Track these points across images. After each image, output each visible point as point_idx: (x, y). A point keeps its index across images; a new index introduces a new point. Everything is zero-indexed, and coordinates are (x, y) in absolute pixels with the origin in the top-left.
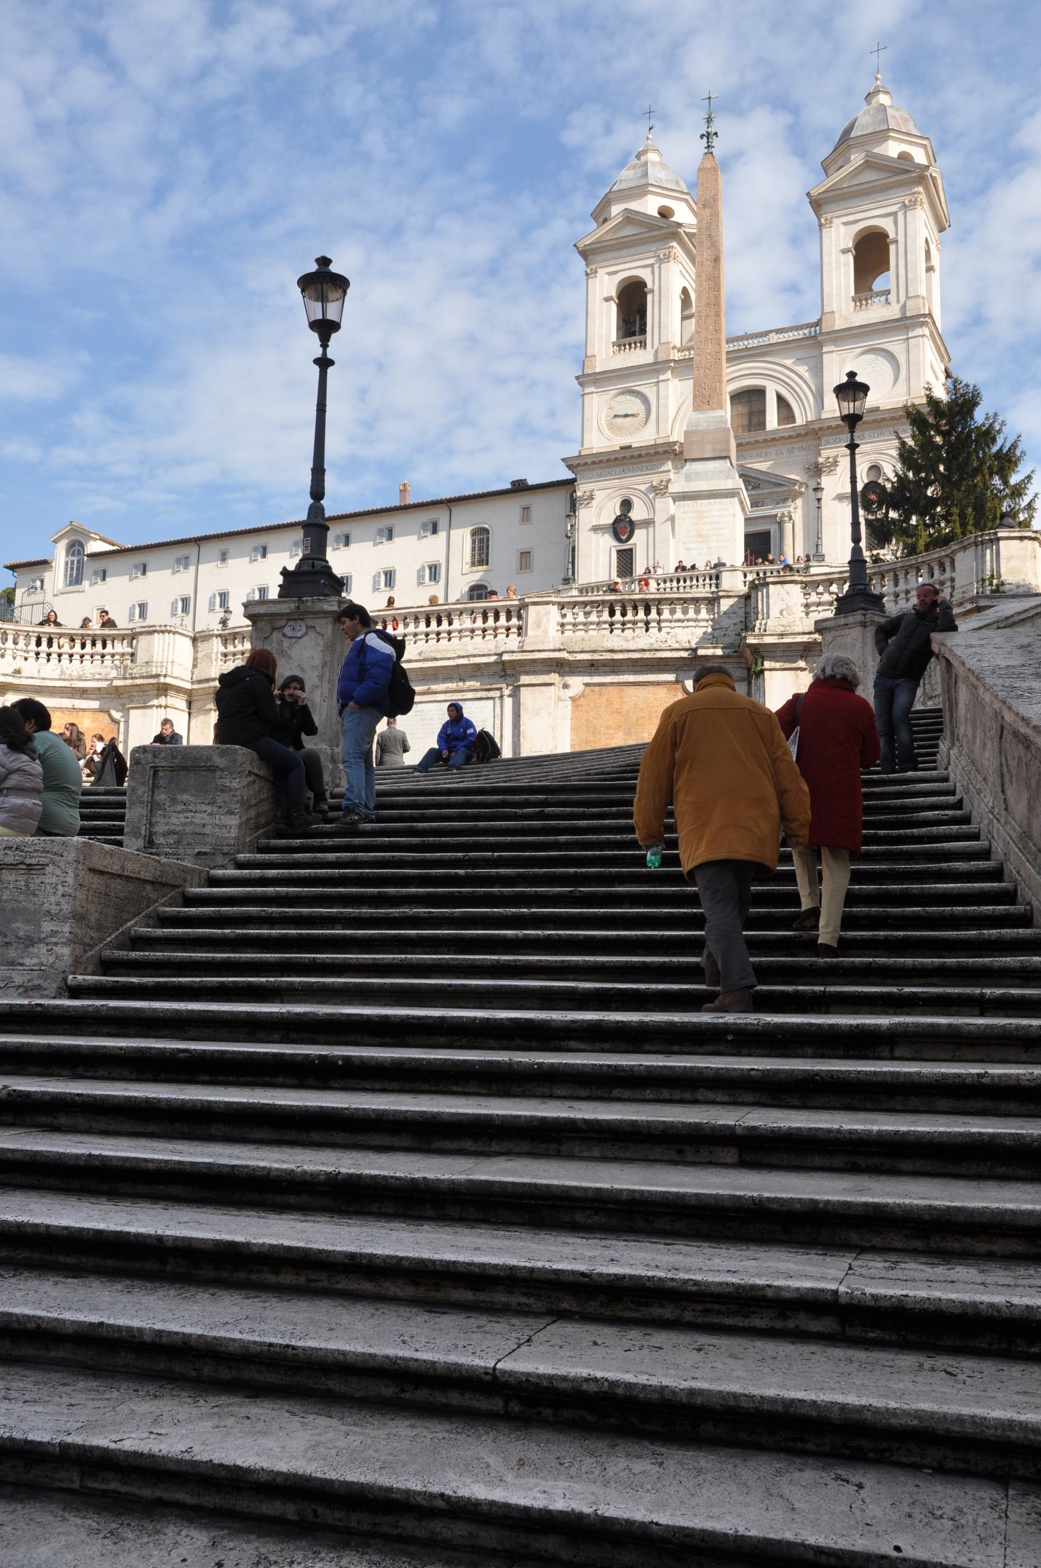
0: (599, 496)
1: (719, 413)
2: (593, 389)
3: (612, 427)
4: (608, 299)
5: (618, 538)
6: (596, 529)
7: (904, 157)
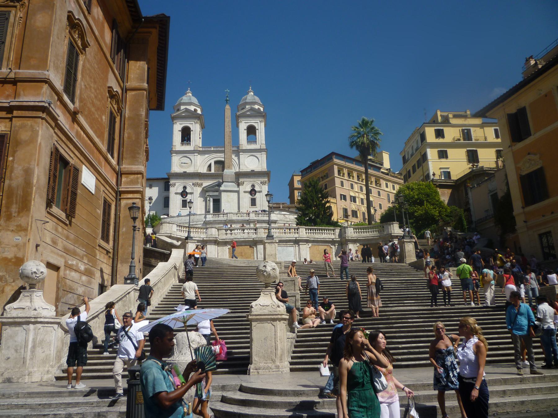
0: (177, 184)
1: (231, 171)
2: (175, 155)
3: (180, 166)
4: (179, 131)
5: (182, 196)
6: (176, 193)
7: (258, 108)
